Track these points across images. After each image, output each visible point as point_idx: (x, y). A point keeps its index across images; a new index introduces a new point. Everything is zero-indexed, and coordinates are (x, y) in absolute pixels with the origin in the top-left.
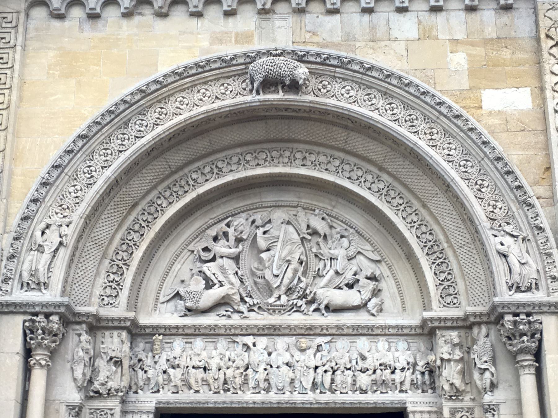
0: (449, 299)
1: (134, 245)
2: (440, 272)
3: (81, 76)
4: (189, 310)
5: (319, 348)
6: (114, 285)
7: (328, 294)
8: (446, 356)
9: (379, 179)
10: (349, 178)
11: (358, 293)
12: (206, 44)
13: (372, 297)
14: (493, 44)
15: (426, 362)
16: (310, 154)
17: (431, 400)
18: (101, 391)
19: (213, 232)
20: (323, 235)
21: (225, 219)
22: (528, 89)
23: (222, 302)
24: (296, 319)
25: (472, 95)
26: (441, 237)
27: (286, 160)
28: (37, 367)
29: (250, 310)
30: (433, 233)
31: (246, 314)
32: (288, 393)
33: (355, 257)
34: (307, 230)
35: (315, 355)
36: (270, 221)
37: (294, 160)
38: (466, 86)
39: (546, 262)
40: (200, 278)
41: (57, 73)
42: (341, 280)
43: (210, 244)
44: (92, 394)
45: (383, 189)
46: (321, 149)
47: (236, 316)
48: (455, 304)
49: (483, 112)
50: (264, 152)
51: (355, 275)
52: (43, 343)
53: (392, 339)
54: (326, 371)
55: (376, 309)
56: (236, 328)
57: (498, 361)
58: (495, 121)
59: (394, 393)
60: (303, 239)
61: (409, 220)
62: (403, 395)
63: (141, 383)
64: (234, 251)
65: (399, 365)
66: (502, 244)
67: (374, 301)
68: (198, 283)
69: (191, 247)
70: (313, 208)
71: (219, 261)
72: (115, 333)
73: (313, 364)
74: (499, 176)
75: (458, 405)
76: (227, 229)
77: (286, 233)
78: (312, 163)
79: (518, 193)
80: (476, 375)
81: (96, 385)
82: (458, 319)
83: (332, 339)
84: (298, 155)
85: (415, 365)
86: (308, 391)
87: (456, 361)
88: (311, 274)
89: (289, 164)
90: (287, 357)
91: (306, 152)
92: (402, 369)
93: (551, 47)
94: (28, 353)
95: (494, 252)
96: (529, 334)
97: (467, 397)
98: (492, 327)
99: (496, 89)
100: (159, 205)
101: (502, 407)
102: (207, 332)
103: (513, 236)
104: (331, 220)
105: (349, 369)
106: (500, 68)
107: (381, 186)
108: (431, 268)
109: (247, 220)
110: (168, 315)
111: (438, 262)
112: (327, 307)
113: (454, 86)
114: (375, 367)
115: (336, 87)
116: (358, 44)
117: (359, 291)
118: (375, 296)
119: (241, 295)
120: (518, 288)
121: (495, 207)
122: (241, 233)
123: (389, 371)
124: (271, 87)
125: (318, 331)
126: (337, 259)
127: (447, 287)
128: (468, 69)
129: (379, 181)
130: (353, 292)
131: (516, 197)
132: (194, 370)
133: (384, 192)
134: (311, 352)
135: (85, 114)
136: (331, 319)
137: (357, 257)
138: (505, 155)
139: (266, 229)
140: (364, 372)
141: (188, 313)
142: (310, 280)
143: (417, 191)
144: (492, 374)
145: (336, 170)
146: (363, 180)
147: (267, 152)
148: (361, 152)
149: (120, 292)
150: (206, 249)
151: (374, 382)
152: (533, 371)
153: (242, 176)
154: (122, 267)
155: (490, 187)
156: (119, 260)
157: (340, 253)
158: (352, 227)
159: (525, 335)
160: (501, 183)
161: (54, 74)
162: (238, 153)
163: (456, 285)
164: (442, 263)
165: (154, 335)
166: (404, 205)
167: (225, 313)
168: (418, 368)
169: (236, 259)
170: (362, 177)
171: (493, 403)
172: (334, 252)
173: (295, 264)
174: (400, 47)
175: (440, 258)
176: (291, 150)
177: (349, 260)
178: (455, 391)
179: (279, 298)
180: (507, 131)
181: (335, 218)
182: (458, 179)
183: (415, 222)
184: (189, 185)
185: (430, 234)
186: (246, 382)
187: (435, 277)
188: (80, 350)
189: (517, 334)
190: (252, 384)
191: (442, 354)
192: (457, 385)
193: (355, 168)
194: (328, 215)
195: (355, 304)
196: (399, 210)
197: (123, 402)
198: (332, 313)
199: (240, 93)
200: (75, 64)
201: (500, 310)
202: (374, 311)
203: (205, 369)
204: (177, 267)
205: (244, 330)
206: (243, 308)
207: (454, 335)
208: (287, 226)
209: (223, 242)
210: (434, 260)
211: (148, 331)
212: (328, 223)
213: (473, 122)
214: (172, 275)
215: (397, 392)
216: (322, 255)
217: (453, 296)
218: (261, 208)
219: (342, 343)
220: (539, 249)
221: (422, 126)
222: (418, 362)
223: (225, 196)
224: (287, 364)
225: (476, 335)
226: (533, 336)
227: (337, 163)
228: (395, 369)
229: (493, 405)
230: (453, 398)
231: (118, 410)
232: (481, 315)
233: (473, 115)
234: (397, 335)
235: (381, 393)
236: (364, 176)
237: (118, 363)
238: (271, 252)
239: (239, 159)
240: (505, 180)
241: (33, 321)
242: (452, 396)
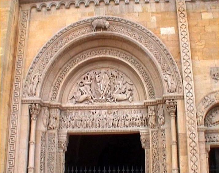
4: (77, 102)
5: (114, 113)
7: (117, 95)
8: (150, 114)
10: (123, 58)
13: (130, 96)
17: (147, 129)
19: (83, 77)
20: (116, 77)
21: (87, 72)
22: (174, 27)
23: (86, 99)
24: (108, 104)
28: (33, 120)
29: (94, 102)
31: (93, 103)
32: (105, 128)
35: (113, 116)
36: (100, 73)
38: (156, 26)
40: (80, 92)
43: (83, 80)
44: (49, 128)
46: (115, 49)
47: (90, 104)
51: (125, 89)
54: (116, 120)
56: (90, 107)
57: (165, 115)
58: (164, 38)
61: (140, 70)
62: (139, 127)
63: (63, 125)
64: (89, 83)
65: (137, 118)
66: (166, 77)
67: (130, 97)
68: (79, 93)
69: (77, 82)
71: (85, 86)
72: (55, 109)
73: (112, 118)
74: (165, 55)
75: (154, 130)
76: (87, 76)
77: (105, 76)
79: (171, 61)
80: (159, 120)
81: (50, 126)
82: (154, 102)
84: (108, 51)
86: (111, 127)
87: (153, 116)
88: (112, 89)
90: (105, 116)
93: (180, 14)
94: (30, 116)
95: (164, 80)
96: (173, 106)
97: (157, 127)
98: (163, 104)
101: (166, 130)
102: (81, 109)
103: (169, 75)
105: (123, 120)
106: (166, 21)
109: (94, 72)
110: (71, 104)
111: (149, 84)
112: (117, 100)
113: (152, 27)
115: (118, 28)
118: (131, 96)
119: (91, 97)
120: (170, 91)
121: (164, 65)
122: (92, 77)
123: (134, 120)
125: (114, 108)
131: (170, 62)
132: (78, 121)
134: (112, 115)
136: (118, 104)
138: (167, 49)
139: (99, 75)
141: (76, 103)
142: (112, 91)
143: (143, 61)
144: (163, 119)
146: (127, 58)
148: (126, 48)
150: (82, 82)
151: (130, 124)
152: (174, 118)
157: (120, 82)
159: (172, 106)
160: (166, 58)
167: (87, 102)
168: (143, 119)
169: (90, 85)
172: (119, 82)
173: (107, 86)
179: (103, 97)
180: (168, 41)
182: (153, 57)
186: (93, 125)
189: (170, 106)
190: (94, 125)
192: (153, 123)
197: (58, 131)
202: (131, 101)
203: (81, 120)
204: (73, 88)
206: (92, 101)
207: (153, 108)
209: (86, 79)
211: (65, 109)
212: (117, 73)
213: (158, 38)
214: (72, 91)
215: (137, 126)
219: (121, 112)
221: (143, 40)
224: (105, 119)
226: (174, 107)
231: (56, 133)
232: (160, 101)
233: (157, 36)
237: (56, 119)
238: (101, 83)
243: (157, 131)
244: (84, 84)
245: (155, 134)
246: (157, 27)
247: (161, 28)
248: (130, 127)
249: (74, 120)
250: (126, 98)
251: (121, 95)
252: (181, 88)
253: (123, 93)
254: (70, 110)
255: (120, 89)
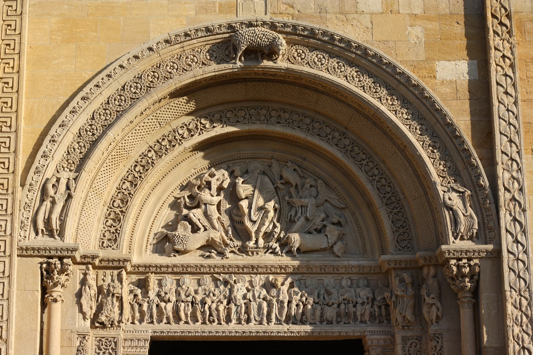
0: (404, 244)
1: (128, 193)
2: (396, 220)
3: (80, 42)
6: (113, 230)
9: (345, 136)
10: (319, 135)
11: (326, 238)
12: (192, 13)
14: (446, 19)
15: (382, 297)
16: (284, 112)
18: (105, 323)
20: (294, 184)
22: (476, 61)
25: (427, 66)
26: (398, 189)
27: (263, 118)
30: (392, 185)
33: (323, 204)
34: (280, 180)
37: (270, 118)
38: (422, 57)
39: (485, 215)
41: (59, 38)
42: (311, 225)
45: (348, 146)
48: (408, 248)
49: (437, 81)
50: (243, 110)
51: (323, 221)
52: (52, 282)
53: (355, 277)
55: (340, 252)
59: (355, 323)
60: (276, 188)
61: (370, 174)
65: (360, 300)
66: (450, 199)
67: (339, 244)
70: (286, 160)
74: (448, 139)
75: (409, 334)
78: (286, 121)
80: (425, 310)
83: (303, 277)
84: (274, 113)
85: (374, 299)
89: (266, 122)
91: (280, 111)
92: (362, 303)
99: (449, 61)
100: (150, 158)
104: (302, 171)
105: (318, 303)
107: (347, 142)
108: (389, 217)
111: (395, 211)
113: (412, 57)
114: (339, 302)
116: (328, 16)
117: (326, 235)
123: (351, 305)
124: (251, 55)
126: (307, 207)
127: (402, 233)
128: (425, 41)
129: (345, 138)
130: (322, 235)
133: (349, 148)
135: (85, 77)
137: (324, 204)
140: (330, 306)
144: (438, 309)
145: (307, 127)
146: (330, 137)
147: (246, 110)
149: (117, 236)
151: (338, 315)
153: (223, 132)
154: (118, 214)
155: (441, 148)
156: (116, 207)
158: (320, 178)
161: (55, 39)
162: (220, 111)
163: (410, 231)
164: (398, 212)
165: (148, 273)
166: (366, 161)
168: (376, 303)
170: (330, 134)
171: (438, 332)
172: (305, 201)
174: (366, 20)
175: (397, 208)
176: (267, 109)
177: (317, 207)
178: (407, 321)
181: (305, 169)
183: (376, 176)
184: (176, 140)
185: (389, 186)
187: (392, 225)
188: (87, 287)
190: (234, 316)
191: (397, 291)
192: (408, 317)
193: (324, 127)
194: (299, 166)
195: (322, 247)
196: (363, 164)
198: (303, 255)
199: (223, 59)
200: (75, 30)
201: (447, 255)
205: (226, 270)
208: (263, 176)
210: (392, 209)
216: (294, 203)
217: (407, 242)
218: (239, 159)
220: (479, 204)
222: (376, 297)
223: (207, 149)
225: (426, 274)
227: (308, 121)
228: (357, 303)
229: (438, 334)
230: (405, 328)
234: (358, 274)
235: (345, 323)
236: (331, 134)
239: (221, 116)
240: (453, 142)
241: (48, 264)
242: (405, 326)
243: (419, 338)
244: (199, 202)
245: (413, 345)
246: (427, 59)
247: (438, 60)
248: (338, 322)
249: (169, 301)
250: (324, 245)
251: (311, 236)
252: (491, 229)
253: (316, 230)
254: (156, 273)
255: (307, 219)
